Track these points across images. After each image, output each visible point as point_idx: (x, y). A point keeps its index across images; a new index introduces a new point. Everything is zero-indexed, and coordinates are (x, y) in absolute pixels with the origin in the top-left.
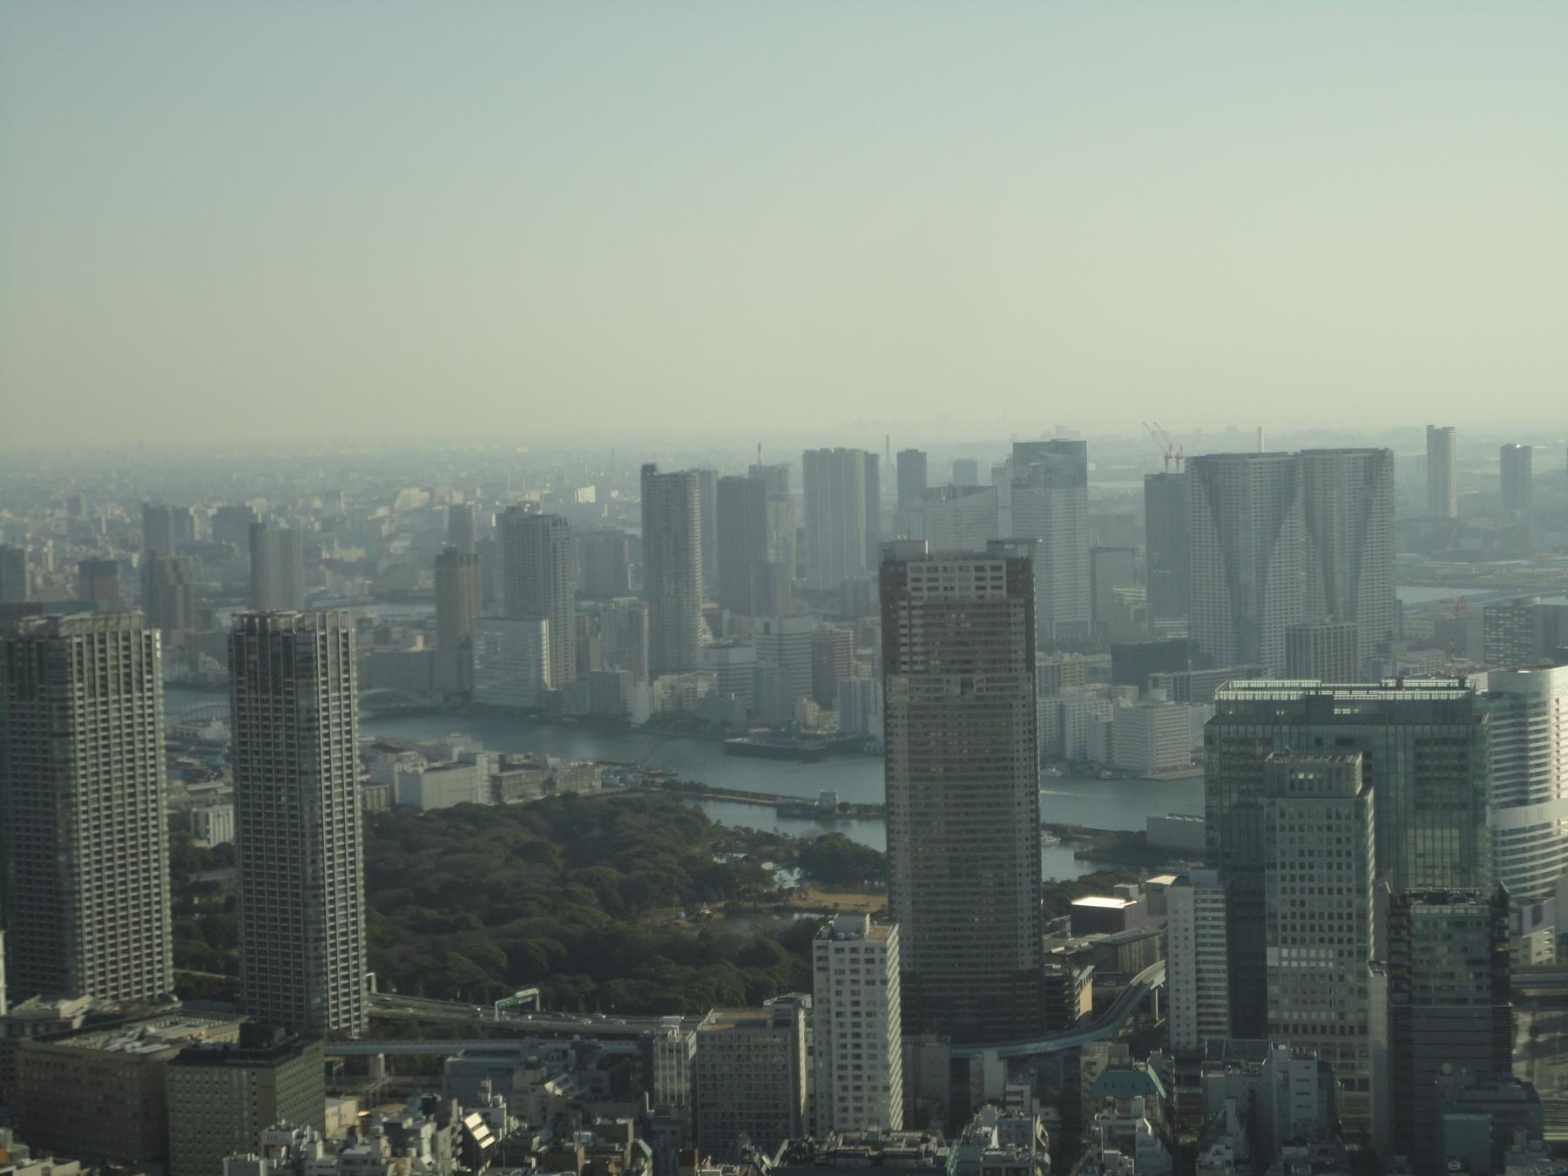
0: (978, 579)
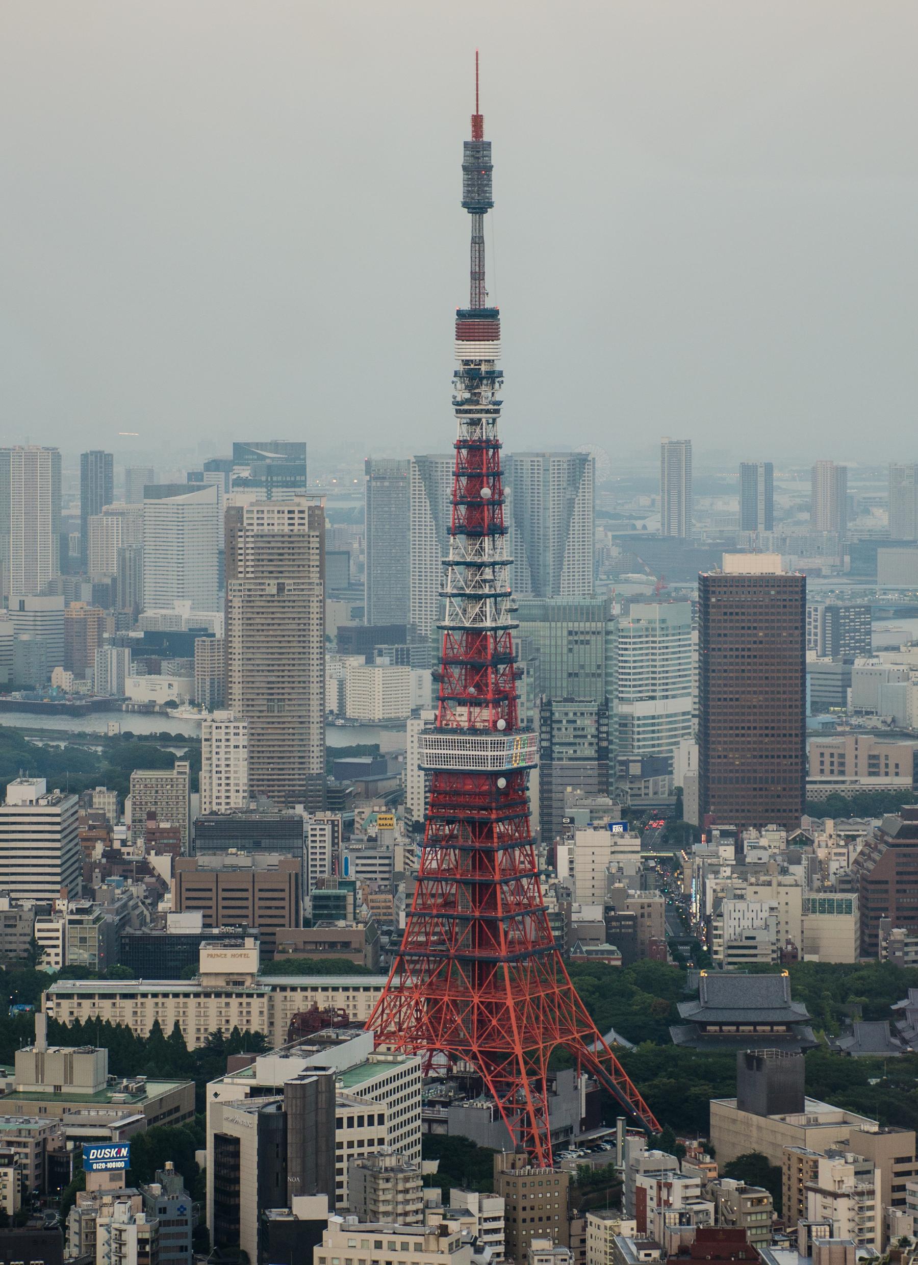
0: (289, 519)
